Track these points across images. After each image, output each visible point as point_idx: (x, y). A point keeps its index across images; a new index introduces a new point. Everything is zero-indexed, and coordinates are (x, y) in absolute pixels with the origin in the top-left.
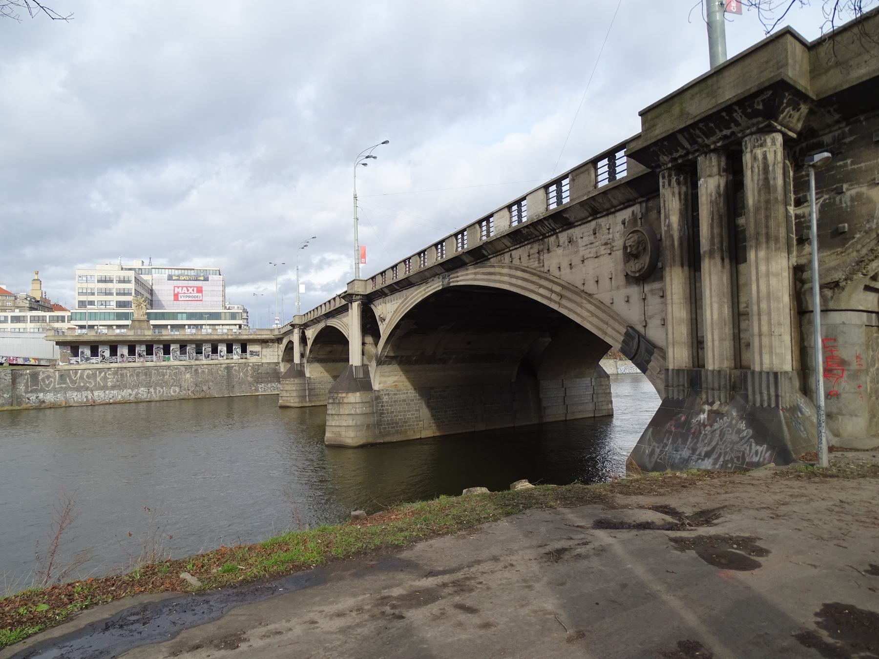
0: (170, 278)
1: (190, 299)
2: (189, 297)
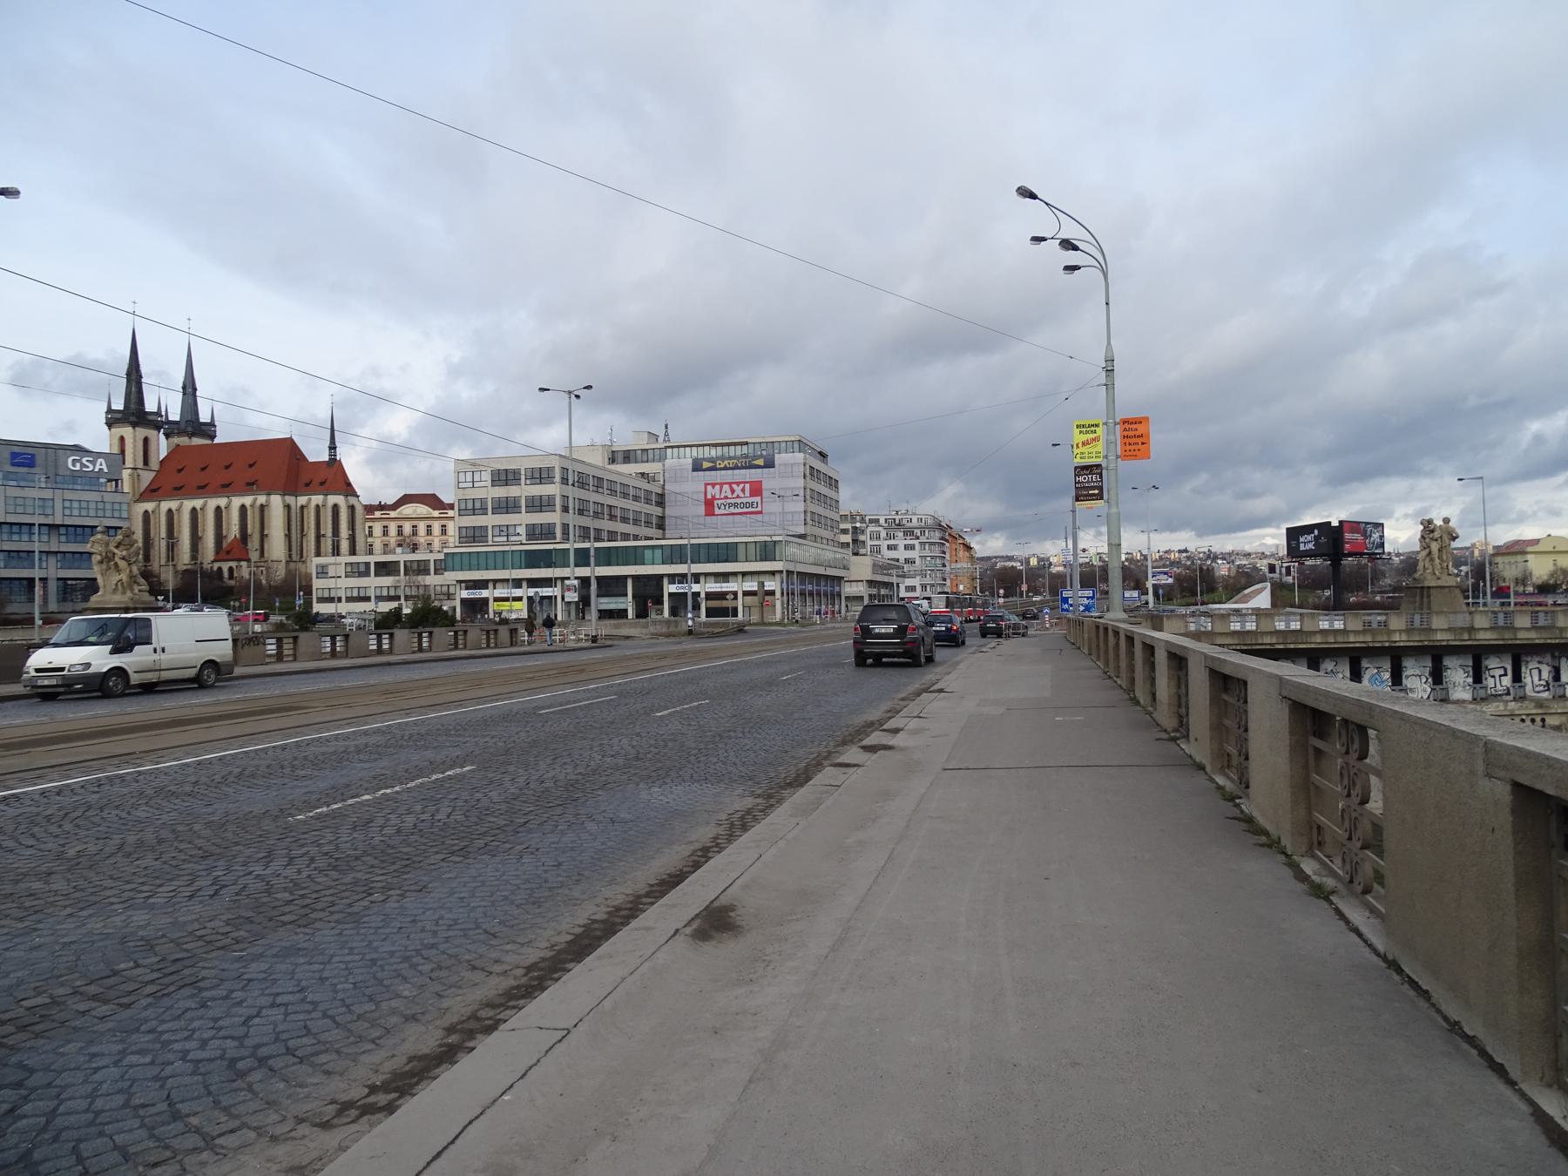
0: (697, 466)
1: (736, 511)
2: (736, 505)
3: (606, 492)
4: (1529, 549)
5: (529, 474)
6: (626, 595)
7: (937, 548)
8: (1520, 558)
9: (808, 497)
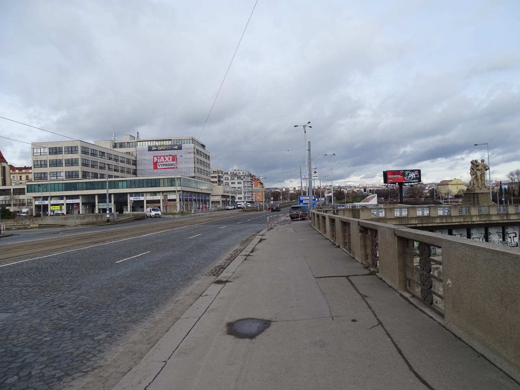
3: (106, 158)
4: (449, 183)
5: (66, 150)
7: (250, 183)
8: (446, 186)
9: (196, 162)
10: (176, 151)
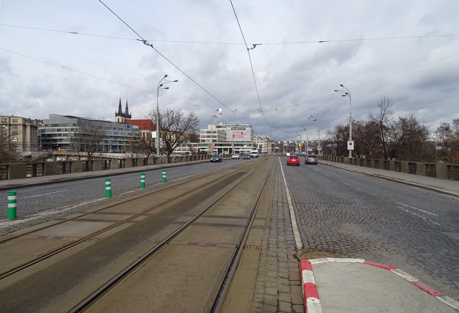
2: (239, 136)
6: (228, 151)
10: (243, 130)
